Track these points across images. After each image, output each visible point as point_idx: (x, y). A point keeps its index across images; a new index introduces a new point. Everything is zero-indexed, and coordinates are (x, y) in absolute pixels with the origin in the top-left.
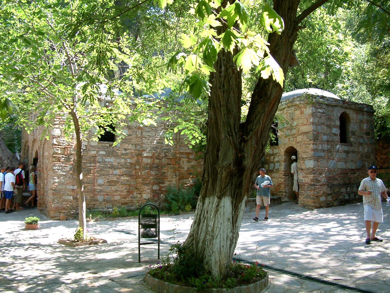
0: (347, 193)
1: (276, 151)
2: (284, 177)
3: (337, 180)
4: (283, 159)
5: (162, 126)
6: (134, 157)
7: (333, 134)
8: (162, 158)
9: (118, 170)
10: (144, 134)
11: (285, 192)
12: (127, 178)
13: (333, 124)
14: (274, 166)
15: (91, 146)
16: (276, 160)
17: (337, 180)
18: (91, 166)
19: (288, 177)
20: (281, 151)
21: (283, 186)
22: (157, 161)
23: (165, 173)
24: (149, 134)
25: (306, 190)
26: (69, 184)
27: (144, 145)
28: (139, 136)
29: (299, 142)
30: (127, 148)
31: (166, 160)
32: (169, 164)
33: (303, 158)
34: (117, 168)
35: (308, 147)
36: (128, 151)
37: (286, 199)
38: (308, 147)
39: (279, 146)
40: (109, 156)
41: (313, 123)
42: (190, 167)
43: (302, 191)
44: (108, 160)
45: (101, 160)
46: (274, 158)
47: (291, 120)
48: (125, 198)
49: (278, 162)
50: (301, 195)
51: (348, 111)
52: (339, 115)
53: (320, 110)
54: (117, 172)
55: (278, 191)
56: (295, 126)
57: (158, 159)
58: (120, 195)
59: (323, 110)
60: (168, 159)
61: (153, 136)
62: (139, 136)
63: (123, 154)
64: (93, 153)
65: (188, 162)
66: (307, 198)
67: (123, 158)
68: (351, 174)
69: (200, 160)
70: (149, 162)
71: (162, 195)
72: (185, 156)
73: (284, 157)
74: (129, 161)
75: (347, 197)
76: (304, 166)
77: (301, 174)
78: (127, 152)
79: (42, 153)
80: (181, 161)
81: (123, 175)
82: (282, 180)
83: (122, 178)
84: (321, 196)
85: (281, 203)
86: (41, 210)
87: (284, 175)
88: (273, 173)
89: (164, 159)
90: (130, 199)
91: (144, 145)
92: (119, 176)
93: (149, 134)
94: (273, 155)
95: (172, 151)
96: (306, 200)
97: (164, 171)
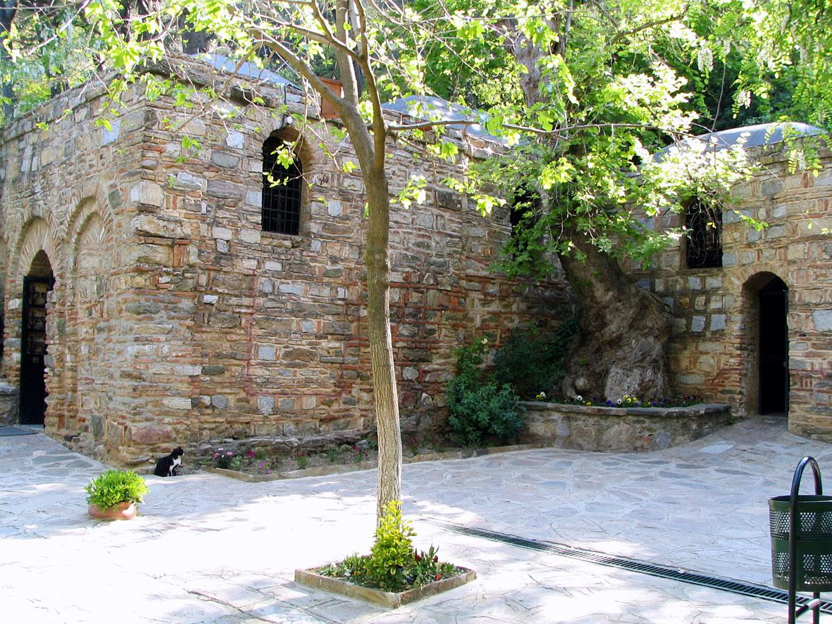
1: (713, 282)
2: (739, 352)
4: (739, 304)
6: (355, 284)
8: (428, 289)
11: (741, 393)
12: (337, 345)
14: (708, 324)
15: (241, 243)
16: (714, 305)
18: (239, 306)
19: (746, 353)
20: (731, 283)
21: (735, 376)
22: (415, 297)
23: (432, 332)
25: (815, 389)
26: (183, 359)
29: (794, 262)
30: (337, 254)
33: (808, 304)
35: (824, 275)
36: (340, 266)
37: (742, 412)
38: (824, 275)
39: (725, 270)
40: (291, 277)
42: (487, 317)
43: (802, 393)
44: (286, 288)
45: (268, 289)
46: (708, 301)
47: (768, 202)
48: (329, 404)
49: (720, 311)
50: (799, 403)
54: (311, 325)
55: (720, 389)
56: (780, 219)
57: (417, 290)
58: (316, 394)
63: (326, 274)
64: (248, 265)
65: (485, 303)
66: (819, 413)
67: (328, 284)
69: (512, 299)
71: (424, 395)
72: (476, 285)
73: (740, 298)
74: (342, 293)
76: (811, 325)
77: (801, 346)
79: (72, 261)
80: (468, 300)
81: (324, 337)
82: (732, 360)
85: (730, 422)
86: (68, 438)
87: (740, 349)
88: (704, 341)
89: (431, 292)
90: (343, 406)
94: (703, 292)
95: (451, 270)
96: (815, 417)
97: (429, 327)
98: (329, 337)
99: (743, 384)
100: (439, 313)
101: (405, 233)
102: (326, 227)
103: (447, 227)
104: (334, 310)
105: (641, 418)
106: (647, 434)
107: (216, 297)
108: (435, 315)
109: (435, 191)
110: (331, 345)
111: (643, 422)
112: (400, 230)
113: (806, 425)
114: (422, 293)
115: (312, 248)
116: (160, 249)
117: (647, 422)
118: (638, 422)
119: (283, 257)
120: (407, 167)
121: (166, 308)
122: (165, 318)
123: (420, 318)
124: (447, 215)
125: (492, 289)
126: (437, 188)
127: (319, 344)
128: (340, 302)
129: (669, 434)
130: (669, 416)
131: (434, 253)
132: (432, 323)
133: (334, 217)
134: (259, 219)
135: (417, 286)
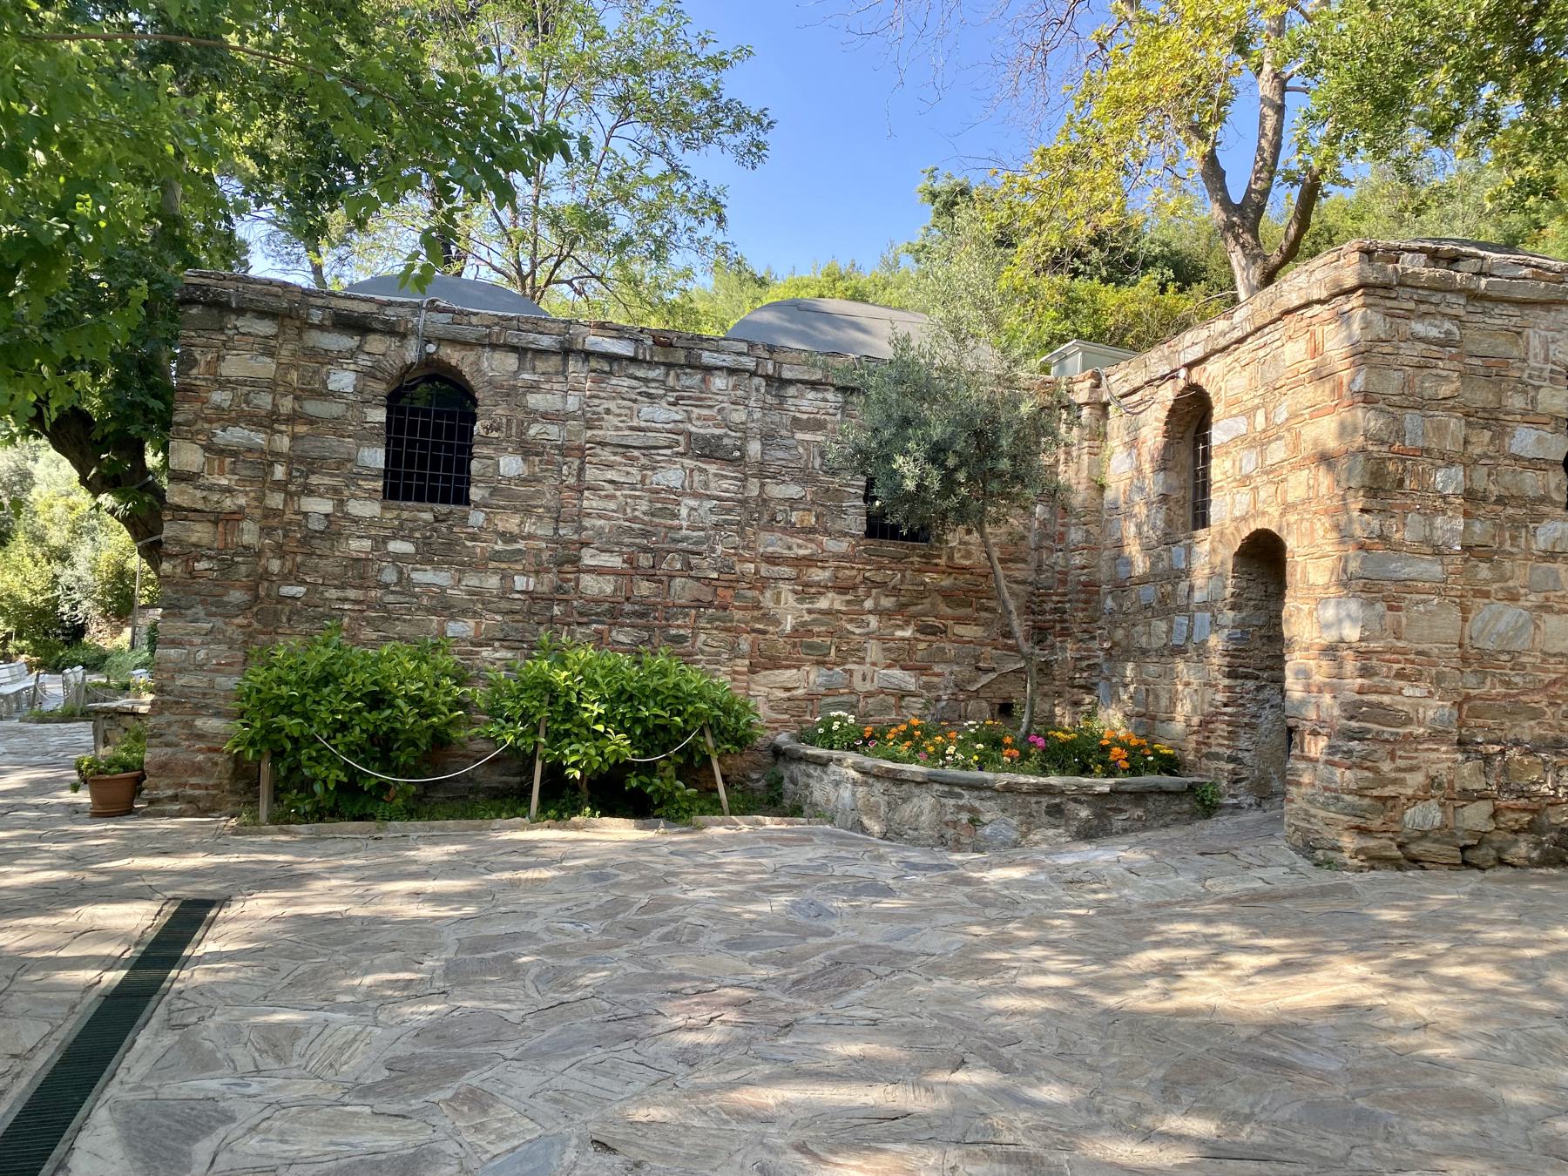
2: (1227, 682)
3: (1536, 714)
6: (548, 571)
7: (1517, 458)
8: (671, 577)
9: (471, 623)
10: (591, 474)
12: (510, 655)
13: (1516, 402)
15: (347, 516)
17: (1536, 714)
18: (345, 600)
22: (644, 588)
23: (683, 638)
24: (610, 475)
27: (587, 522)
28: (572, 481)
30: (516, 530)
31: (691, 583)
32: (698, 604)
34: (464, 612)
36: (521, 545)
40: (431, 562)
42: (807, 618)
44: (425, 576)
53: (1419, 328)
54: (461, 628)
57: (650, 578)
59: (1447, 325)
60: (698, 579)
61: (633, 487)
62: (572, 481)
63: (497, 556)
64: (359, 546)
67: (496, 571)
70: (609, 589)
74: (520, 582)
78: (518, 546)
81: (488, 643)
83: (486, 653)
84: (1413, 800)
91: (587, 522)
92: (473, 644)
93: (610, 475)
97: (673, 632)
98: (497, 644)
99: (1243, 744)
100: (694, 611)
101: (626, 496)
102: (494, 492)
103: (712, 485)
104: (504, 605)
105: (957, 790)
106: (964, 817)
107: (303, 589)
108: (687, 615)
109: (691, 433)
110: (497, 655)
111: (960, 796)
112: (618, 493)
113: (1309, 830)
114: (660, 582)
116: (198, 527)
117: (968, 798)
119: (417, 535)
120: (635, 401)
121: (203, 602)
122: (202, 614)
124: (712, 468)
125: (819, 575)
126: (693, 429)
127: (478, 653)
128: (517, 596)
129: (1014, 822)
130: (1009, 789)
131: (685, 524)
132: (679, 627)
133: (510, 479)
134: (379, 485)
135: (652, 571)
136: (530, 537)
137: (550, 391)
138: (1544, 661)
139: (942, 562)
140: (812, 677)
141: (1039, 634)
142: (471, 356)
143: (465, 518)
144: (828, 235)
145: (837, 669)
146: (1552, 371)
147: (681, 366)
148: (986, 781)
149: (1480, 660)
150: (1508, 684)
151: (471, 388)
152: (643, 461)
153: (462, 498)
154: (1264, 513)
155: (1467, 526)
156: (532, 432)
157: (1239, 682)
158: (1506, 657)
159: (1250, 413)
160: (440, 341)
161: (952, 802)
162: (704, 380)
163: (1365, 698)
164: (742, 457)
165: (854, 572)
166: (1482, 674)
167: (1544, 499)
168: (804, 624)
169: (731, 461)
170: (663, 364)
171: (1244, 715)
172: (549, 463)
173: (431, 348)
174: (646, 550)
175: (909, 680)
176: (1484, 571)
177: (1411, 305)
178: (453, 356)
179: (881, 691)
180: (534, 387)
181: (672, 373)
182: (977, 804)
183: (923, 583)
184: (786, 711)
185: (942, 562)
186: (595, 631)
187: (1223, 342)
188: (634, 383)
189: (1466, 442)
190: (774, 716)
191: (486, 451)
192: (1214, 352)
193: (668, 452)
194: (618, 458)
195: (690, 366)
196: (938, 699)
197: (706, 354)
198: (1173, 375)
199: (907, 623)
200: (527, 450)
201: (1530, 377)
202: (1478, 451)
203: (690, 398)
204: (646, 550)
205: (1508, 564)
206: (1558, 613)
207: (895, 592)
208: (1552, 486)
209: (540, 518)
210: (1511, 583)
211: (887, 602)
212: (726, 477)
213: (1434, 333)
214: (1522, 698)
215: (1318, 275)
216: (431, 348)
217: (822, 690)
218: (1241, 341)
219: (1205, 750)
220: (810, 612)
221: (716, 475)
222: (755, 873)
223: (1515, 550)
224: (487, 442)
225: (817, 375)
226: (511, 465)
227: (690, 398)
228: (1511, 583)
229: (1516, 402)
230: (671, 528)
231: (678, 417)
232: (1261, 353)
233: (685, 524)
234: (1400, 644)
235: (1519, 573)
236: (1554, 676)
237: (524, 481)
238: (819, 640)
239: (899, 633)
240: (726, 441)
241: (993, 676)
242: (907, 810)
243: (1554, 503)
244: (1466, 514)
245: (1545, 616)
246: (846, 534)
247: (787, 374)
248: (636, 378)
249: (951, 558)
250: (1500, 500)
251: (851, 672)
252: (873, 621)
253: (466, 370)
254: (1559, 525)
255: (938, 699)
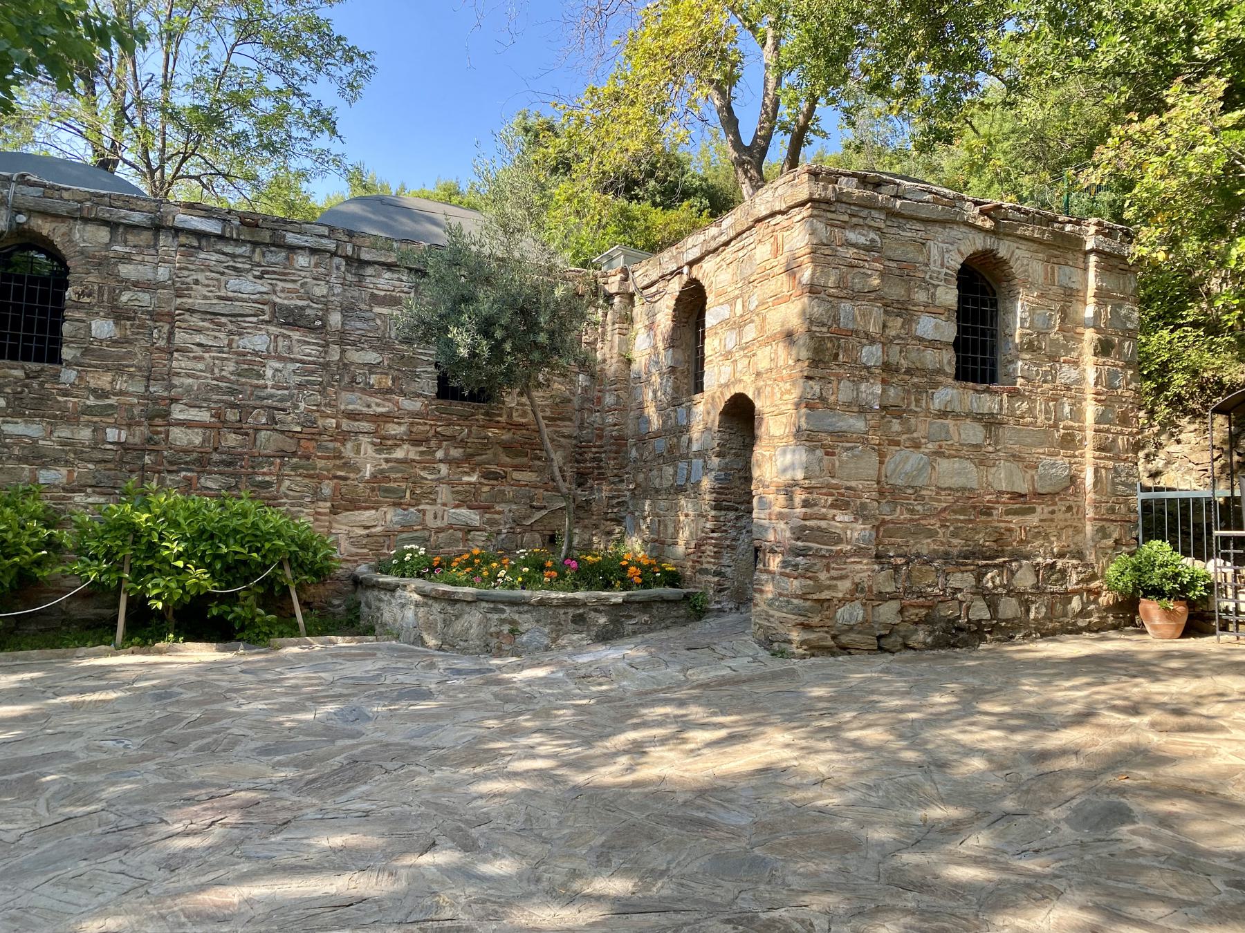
0: (980, 591)
2: (713, 513)
3: (931, 534)
5: (263, 312)
6: (139, 424)
7: (921, 339)
8: (257, 430)
9: (64, 471)
10: (180, 337)
12: (102, 500)
13: (921, 296)
17: (931, 534)
22: (232, 440)
23: (270, 484)
24: (198, 339)
27: (176, 381)
28: (162, 343)
30: (108, 387)
31: (276, 435)
32: (282, 454)
34: (56, 461)
40: (22, 415)
41: (813, 290)
42: (384, 466)
51: (1004, 249)
52: (956, 262)
53: (852, 236)
57: (237, 431)
59: (872, 235)
60: (283, 432)
62: (162, 343)
63: (88, 410)
68: (1008, 513)
70: (197, 440)
74: (112, 434)
75: (980, 611)
81: (80, 489)
83: (78, 498)
84: (843, 601)
89: (263, 434)
91: (176, 381)
92: (65, 489)
93: (198, 339)
98: (89, 490)
99: (725, 561)
100: (278, 461)
101: (214, 358)
102: (86, 352)
103: (296, 350)
104: (98, 455)
105: (501, 606)
106: (506, 628)
108: (272, 463)
109: (275, 304)
110: (90, 500)
111: (503, 611)
112: (206, 355)
114: (247, 434)
115: (62, 379)
117: (509, 612)
118: (495, 610)
119: (8, 390)
120: (223, 274)
123: (242, 467)
124: (296, 335)
125: (394, 429)
126: (278, 300)
129: (546, 630)
130: (542, 603)
131: (270, 383)
132: (264, 474)
133: (101, 341)
135: (238, 425)
136: (122, 393)
137: (141, 263)
138: (937, 494)
139: (503, 419)
140: (389, 517)
141: (581, 479)
142: (62, 228)
143: (57, 376)
144: (414, 149)
145: (412, 509)
146: (946, 274)
147: (267, 245)
148: (524, 597)
149: (892, 493)
150: (912, 511)
151: (63, 256)
152: (230, 327)
153: (55, 358)
154: (740, 381)
155: (884, 391)
156: (124, 298)
157: (723, 513)
158: (910, 491)
159: (732, 302)
160: (30, 212)
161: (496, 616)
162: (287, 258)
163: (807, 523)
164: (324, 326)
165: (428, 428)
166: (894, 504)
167: (940, 371)
168: (382, 471)
169: (313, 329)
170: (249, 242)
171: (726, 539)
172: (139, 327)
173: (22, 218)
174: (233, 406)
175: (474, 518)
176: (896, 425)
177: (846, 218)
178: (45, 227)
179: (451, 527)
180: (126, 259)
181: (258, 250)
182: (516, 617)
183: (487, 437)
184: (365, 546)
185: (503, 419)
186: (185, 477)
187: (714, 245)
188: (222, 258)
189: (884, 326)
190: (354, 550)
191: (77, 315)
192: (709, 253)
193: (254, 319)
194: (206, 324)
195: (274, 245)
196: (499, 533)
197: (289, 235)
198: (678, 272)
199: (473, 470)
200: (118, 315)
201: (931, 278)
202: (893, 333)
203: (274, 273)
204: (233, 406)
205: (913, 420)
206: (948, 457)
207: (462, 443)
208: (945, 361)
209: (131, 376)
210: (915, 435)
211: (456, 453)
212: (309, 343)
213: (862, 240)
214: (923, 522)
215: (780, 191)
216: (22, 218)
217: (398, 527)
218: (727, 244)
219: (698, 566)
220: (387, 461)
221: (299, 341)
222: (312, 685)
223: (918, 409)
224: (78, 306)
225: (392, 259)
226: (103, 328)
227: (274, 273)
228: (915, 435)
229: (921, 296)
230: (257, 387)
231: (264, 289)
232: (741, 254)
233: (270, 383)
234: (834, 481)
235: (922, 428)
236: (945, 505)
237: (114, 342)
238: (395, 485)
239: (466, 479)
240: (308, 312)
241: (544, 512)
242: (458, 626)
243: (946, 374)
244: (884, 382)
245: (939, 460)
246: (419, 395)
247: (365, 256)
248: (223, 253)
249: (510, 416)
250: (908, 371)
251: (424, 512)
252: (444, 469)
253: (57, 240)
254: (950, 391)
255: (499, 533)
